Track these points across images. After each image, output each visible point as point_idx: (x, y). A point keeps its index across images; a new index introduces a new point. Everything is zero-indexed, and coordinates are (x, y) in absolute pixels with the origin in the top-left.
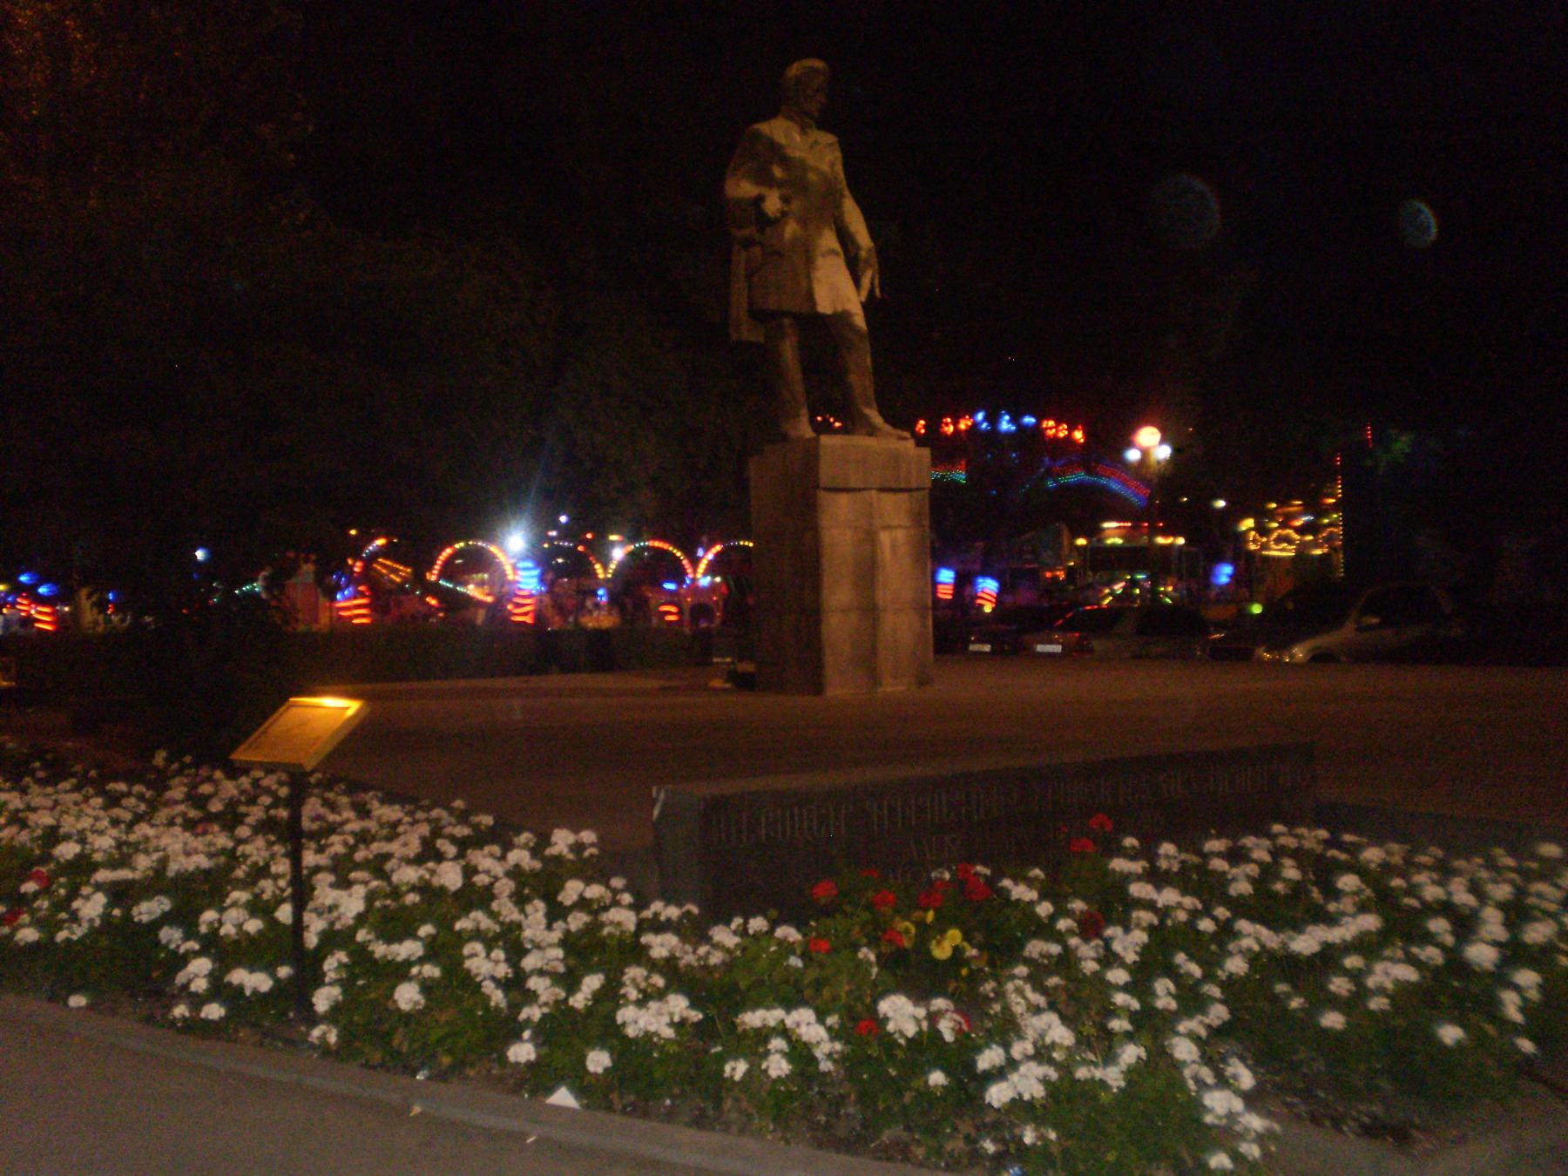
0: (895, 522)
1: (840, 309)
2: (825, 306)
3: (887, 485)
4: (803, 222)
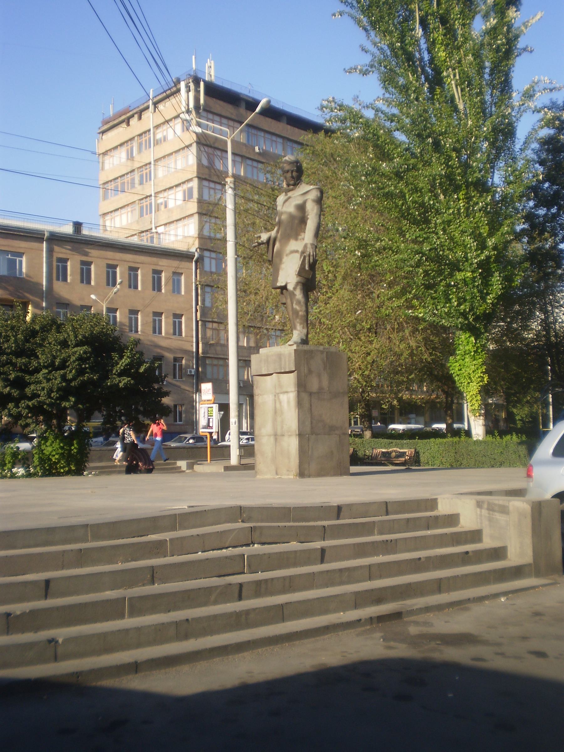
0: (289, 390)
4: (280, 241)
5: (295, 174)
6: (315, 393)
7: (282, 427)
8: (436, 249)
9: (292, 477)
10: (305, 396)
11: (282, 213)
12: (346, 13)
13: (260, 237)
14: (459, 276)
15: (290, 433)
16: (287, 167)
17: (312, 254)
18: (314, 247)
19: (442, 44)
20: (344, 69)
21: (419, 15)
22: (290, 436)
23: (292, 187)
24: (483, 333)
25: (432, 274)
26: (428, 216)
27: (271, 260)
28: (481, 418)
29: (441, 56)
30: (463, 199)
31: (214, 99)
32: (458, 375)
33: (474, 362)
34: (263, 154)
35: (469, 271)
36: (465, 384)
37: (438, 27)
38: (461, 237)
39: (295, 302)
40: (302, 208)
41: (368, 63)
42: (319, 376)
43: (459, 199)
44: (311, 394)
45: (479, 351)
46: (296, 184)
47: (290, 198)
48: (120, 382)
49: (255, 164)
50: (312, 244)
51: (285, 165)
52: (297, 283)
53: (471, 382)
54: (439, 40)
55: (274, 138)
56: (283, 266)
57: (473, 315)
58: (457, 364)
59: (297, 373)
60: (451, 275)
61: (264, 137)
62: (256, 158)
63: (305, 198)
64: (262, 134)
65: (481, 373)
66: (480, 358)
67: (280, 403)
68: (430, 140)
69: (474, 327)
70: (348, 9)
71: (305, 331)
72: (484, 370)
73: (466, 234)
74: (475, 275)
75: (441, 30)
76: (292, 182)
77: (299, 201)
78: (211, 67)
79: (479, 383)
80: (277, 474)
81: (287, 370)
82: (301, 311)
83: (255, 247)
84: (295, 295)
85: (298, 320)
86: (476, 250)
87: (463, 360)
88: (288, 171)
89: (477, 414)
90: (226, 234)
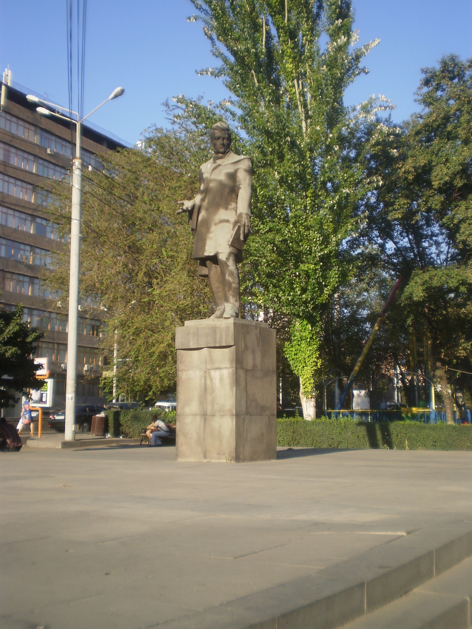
0: (222, 366)
2: (209, 251)
3: (209, 346)
4: (207, 209)
5: (225, 141)
6: (250, 370)
7: (213, 406)
8: (286, 240)
9: (224, 461)
10: (241, 372)
11: (210, 181)
12: (201, 18)
13: (183, 204)
14: (303, 267)
15: (222, 413)
16: (218, 133)
17: (247, 224)
18: (249, 217)
19: (289, 56)
20: (196, 71)
21: (266, 29)
22: (223, 416)
23: (220, 155)
24: (318, 322)
25: (272, 265)
26: (274, 211)
27: (195, 228)
28: (313, 399)
29: (288, 68)
30: (310, 197)
31: (13, 103)
32: (293, 359)
33: (310, 348)
34: (54, 155)
35: (312, 264)
36: (300, 368)
37: (288, 41)
38: (304, 232)
39: (228, 273)
40: (233, 176)
41: (219, 67)
42: (253, 352)
43: (307, 197)
44: (246, 371)
45: (314, 337)
46: (225, 153)
47: (219, 165)
48: (6, 351)
49: (46, 163)
50: (247, 214)
51: (216, 131)
52: (230, 254)
53: (306, 366)
54: (287, 52)
55: (64, 143)
56: (211, 235)
57: (312, 304)
58: (293, 349)
59: (236, 348)
60: (296, 267)
61: (55, 141)
62: (47, 158)
63: (237, 168)
64: (54, 138)
65: (315, 358)
66: (314, 345)
67: (211, 380)
68: (289, 139)
69: (311, 315)
70: (203, 15)
71: (237, 304)
72: (318, 356)
73: (314, 229)
74: (317, 267)
75: (289, 43)
76: (222, 150)
77: (231, 170)
78: (8, 76)
79: (313, 367)
80: (205, 457)
81: (224, 344)
82: (234, 283)
83: (178, 214)
84: (228, 266)
85: (231, 292)
86: (320, 245)
87: (299, 345)
88: (219, 138)
89: (310, 396)
90: (70, 213)
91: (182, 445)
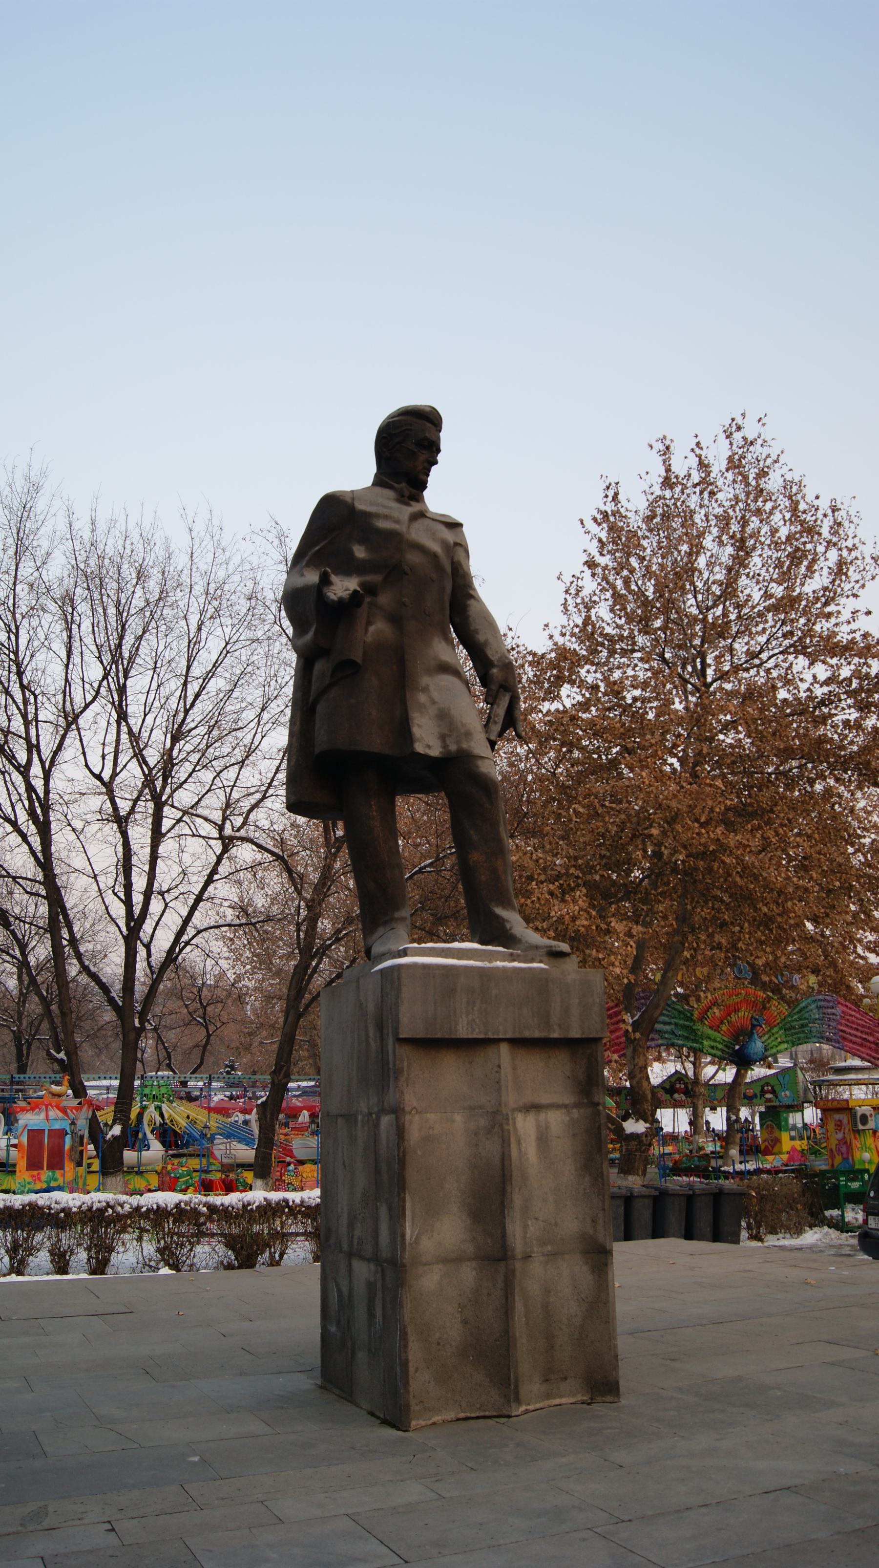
0: (544, 1099)
1: (453, 747)
3: (527, 1034)
4: (396, 620)
7: (525, 1227)
22: (552, 1256)
27: (359, 661)
67: (519, 1142)
77: (449, 536)
91: (417, 1370)
